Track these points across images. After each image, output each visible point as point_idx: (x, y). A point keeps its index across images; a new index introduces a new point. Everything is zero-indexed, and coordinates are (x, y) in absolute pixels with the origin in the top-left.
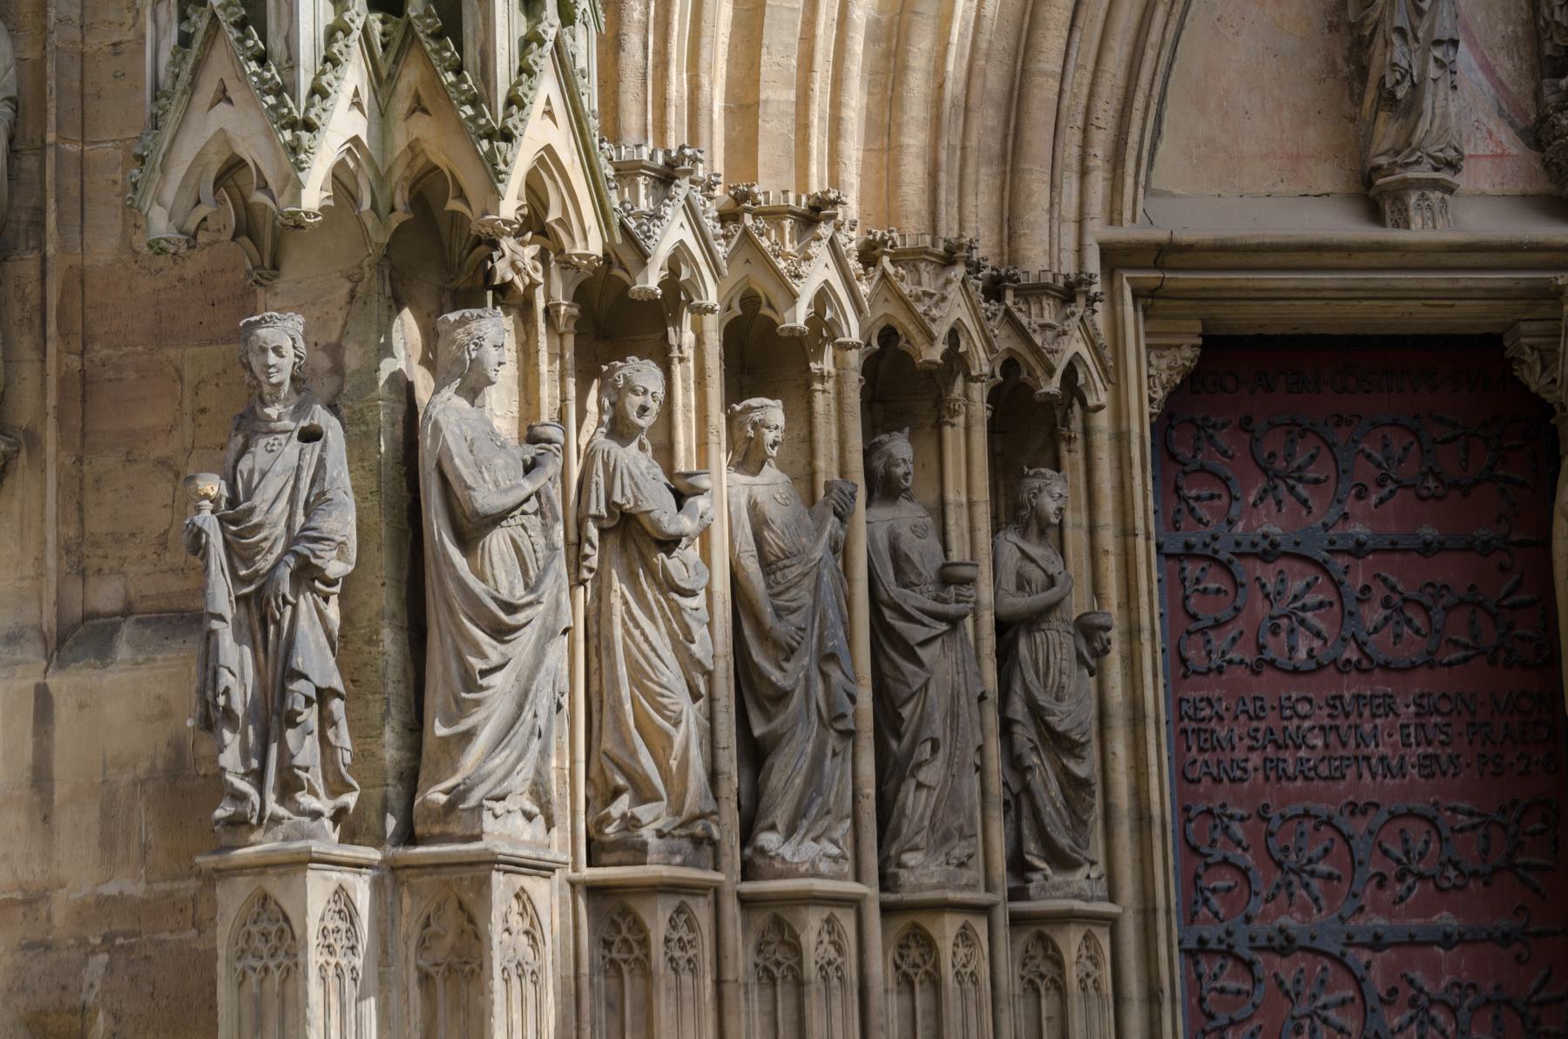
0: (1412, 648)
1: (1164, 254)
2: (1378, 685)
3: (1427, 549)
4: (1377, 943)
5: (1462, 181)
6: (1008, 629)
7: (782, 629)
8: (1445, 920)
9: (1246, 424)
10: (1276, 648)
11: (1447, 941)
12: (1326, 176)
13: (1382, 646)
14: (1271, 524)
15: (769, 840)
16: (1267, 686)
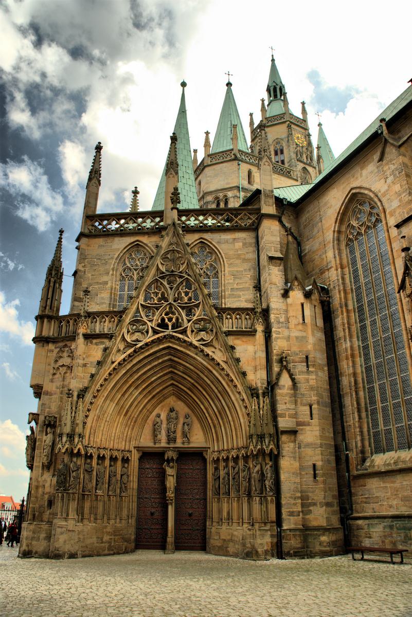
0: (157, 476)
1: (138, 447)
2: (155, 479)
3: (159, 469)
4: (153, 498)
5: (162, 441)
6: (122, 475)
7: (99, 476)
8: (158, 497)
9: (147, 459)
10: (147, 476)
11: (158, 498)
12: (152, 441)
13: (155, 476)
14: (148, 466)
15: (97, 491)
16: (147, 479)
